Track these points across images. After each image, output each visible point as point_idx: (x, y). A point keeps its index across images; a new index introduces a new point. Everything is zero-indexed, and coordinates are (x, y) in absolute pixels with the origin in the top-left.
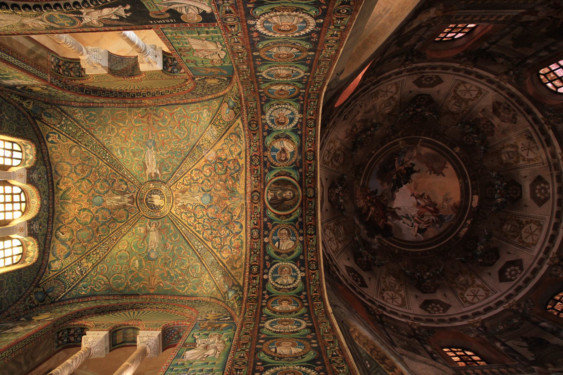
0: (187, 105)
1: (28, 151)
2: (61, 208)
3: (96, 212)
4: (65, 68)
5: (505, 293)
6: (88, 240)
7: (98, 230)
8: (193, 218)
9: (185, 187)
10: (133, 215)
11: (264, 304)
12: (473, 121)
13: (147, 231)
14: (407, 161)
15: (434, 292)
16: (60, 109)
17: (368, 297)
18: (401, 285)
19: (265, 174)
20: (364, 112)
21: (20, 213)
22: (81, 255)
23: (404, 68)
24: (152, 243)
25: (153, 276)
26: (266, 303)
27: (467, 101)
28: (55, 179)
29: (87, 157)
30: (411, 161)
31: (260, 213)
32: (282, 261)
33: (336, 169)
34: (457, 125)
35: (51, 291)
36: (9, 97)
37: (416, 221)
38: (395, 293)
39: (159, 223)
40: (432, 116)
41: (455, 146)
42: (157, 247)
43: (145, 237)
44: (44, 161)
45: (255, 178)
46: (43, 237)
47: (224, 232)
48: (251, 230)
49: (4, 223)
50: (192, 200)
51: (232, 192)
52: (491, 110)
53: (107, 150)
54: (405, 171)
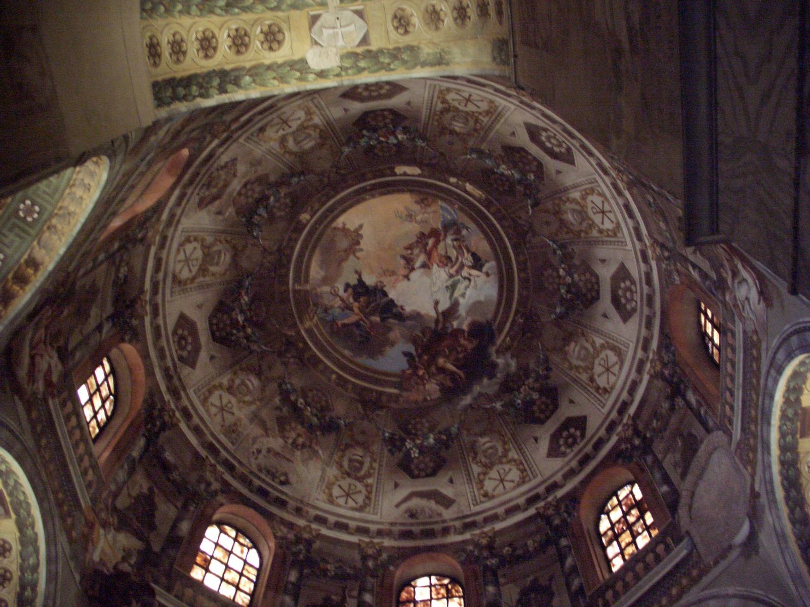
5: (595, 169)
12: (245, 216)
14: (342, 300)
15: (597, 277)
17: (602, 432)
18: (583, 335)
20: (267, 435)
23: (178, 414)
27: (206, 247)
30: (341, 292)
33: (375, 461)
34: (254, 237)
37: (458, 272)
38: (598, 356)
40: (248, 288)
41: (299, 222)
52: (217, 203)
54: (362, 299)
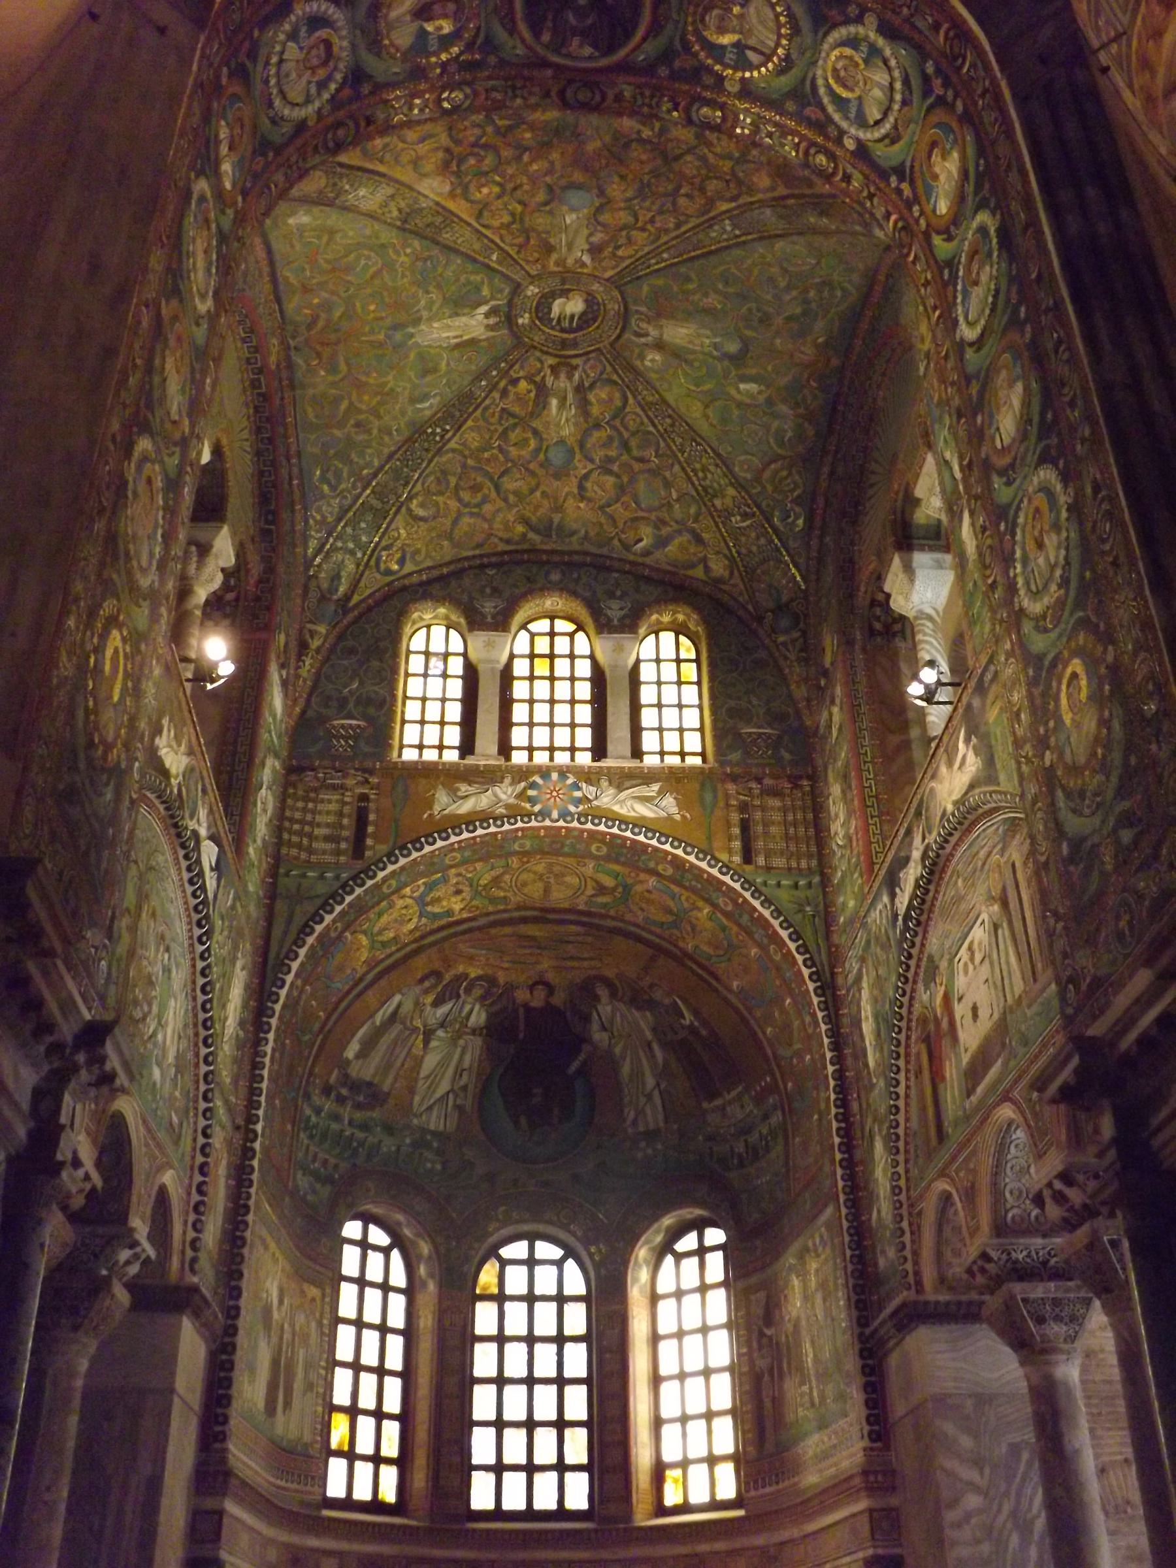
0: (277, 257)
1: (427, 616)
2: (574, 539)
3: (592, 461)
7: (641, 460)
8: (634, 233)
9: (532, 242)
10: (609, 369)
11: (922, 222)
13: (659, 346)
19: (502, 63)
21: (580, 637)
24: (697, 342)
25: (792, 356)
26: (922, 213)
29: (438, 479)
31: (639, 87)
32: (814, 63)
36: (305, 681)
39: (637, 312)
42: (708, 332)
43: (677, 354)
45: (515, 96)
46: (643, 587)
47: (689, 165)
48: (690, 121)
50: (577, 232)
51: (557, 132)
53: (418, 431)
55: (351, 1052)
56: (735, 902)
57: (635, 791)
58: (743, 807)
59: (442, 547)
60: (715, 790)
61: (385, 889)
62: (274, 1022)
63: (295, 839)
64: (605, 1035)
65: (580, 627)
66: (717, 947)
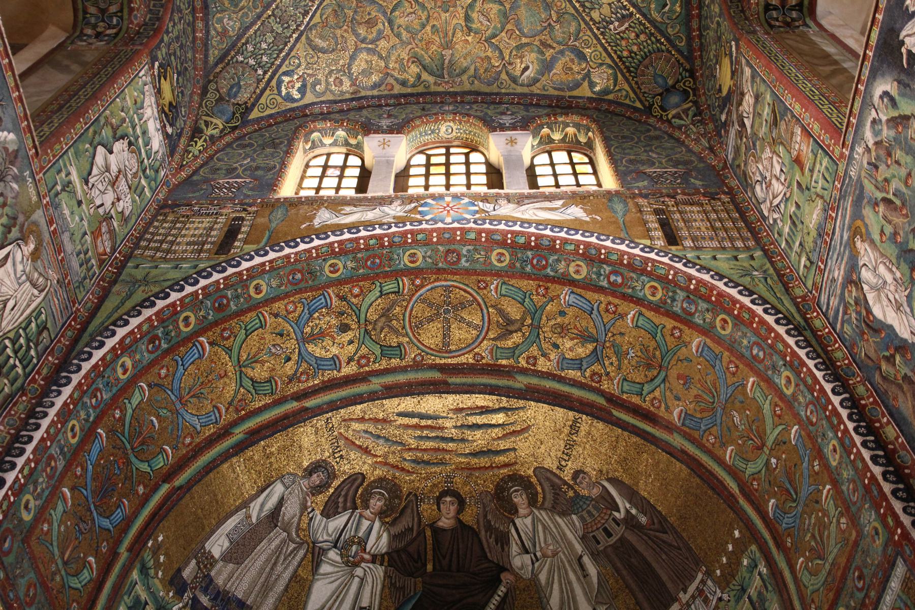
1: (328, 141)
2: (465, 77)
4: (101, 24)
6: (545, 10)
16: (216, 64)
22: (582, 23)
28: (392, 89)
35: (665, 79)
36: (196, 157)
44: (349, 110)
46: (532, 109)
49: (494, 176)
55: (217, 545)
56: (663, 279)
57: (537, 205)
58: (657, 212)
59: (341, 82)
60: (626, 204)
61: (252, 291)
62: (76, 378)
63: (152, 245)
64: (527, 558)
65: (474, 149)
66: (649, 366)
